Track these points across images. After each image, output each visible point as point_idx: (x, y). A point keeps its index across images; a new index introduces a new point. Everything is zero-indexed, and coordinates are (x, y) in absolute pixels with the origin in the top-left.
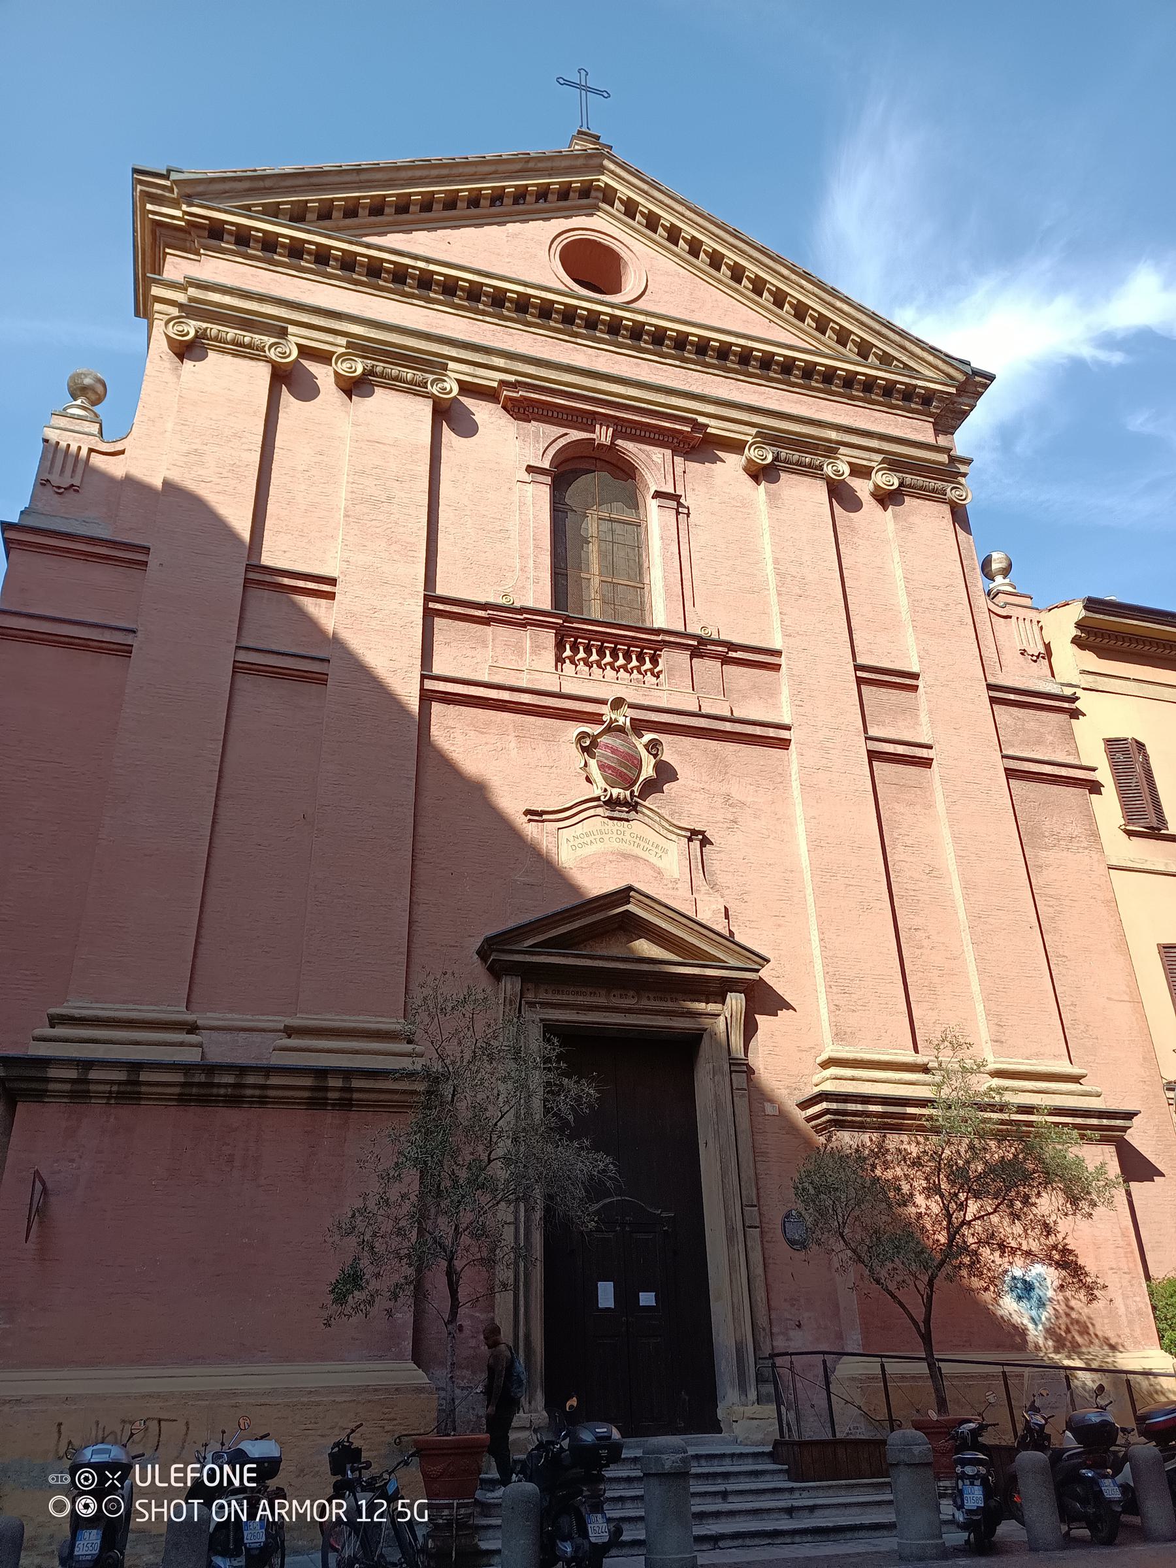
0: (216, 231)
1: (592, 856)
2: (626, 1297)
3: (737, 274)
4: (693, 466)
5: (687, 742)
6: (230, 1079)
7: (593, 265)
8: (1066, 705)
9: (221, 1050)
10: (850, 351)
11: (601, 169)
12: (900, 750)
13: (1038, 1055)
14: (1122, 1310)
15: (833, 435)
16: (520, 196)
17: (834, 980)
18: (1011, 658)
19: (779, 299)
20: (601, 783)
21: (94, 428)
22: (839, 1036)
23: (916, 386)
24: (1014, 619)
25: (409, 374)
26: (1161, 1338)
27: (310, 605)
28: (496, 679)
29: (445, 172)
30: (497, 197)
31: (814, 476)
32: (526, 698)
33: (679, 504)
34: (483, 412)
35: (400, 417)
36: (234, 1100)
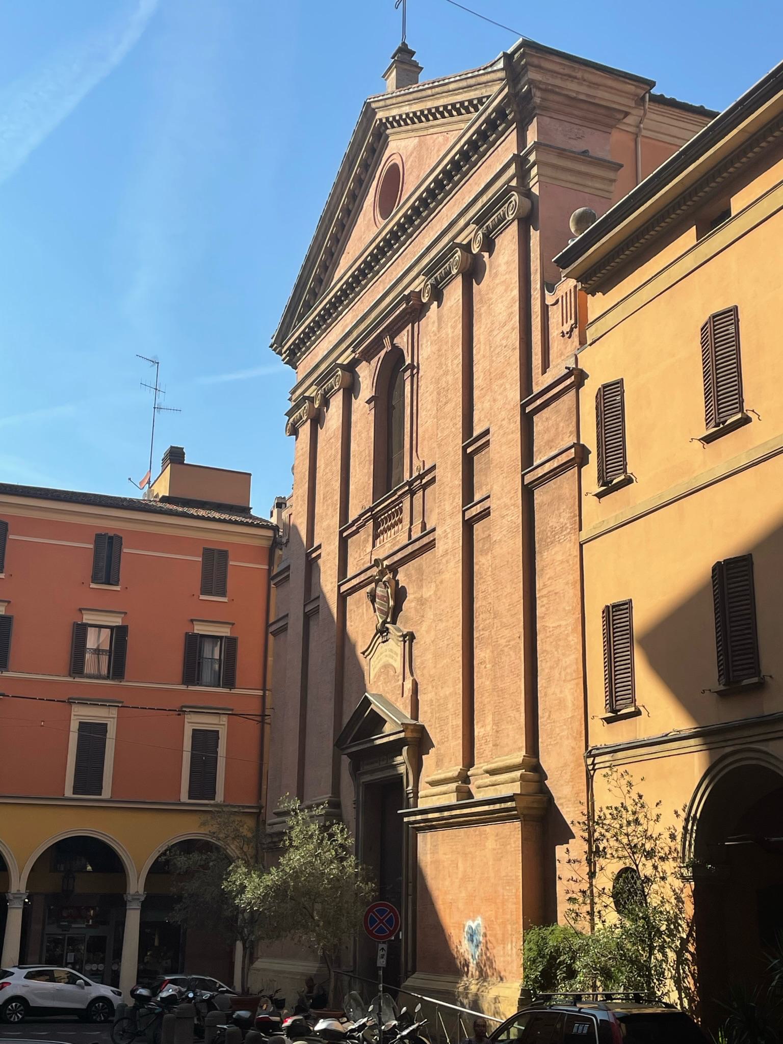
8: (568, 382)
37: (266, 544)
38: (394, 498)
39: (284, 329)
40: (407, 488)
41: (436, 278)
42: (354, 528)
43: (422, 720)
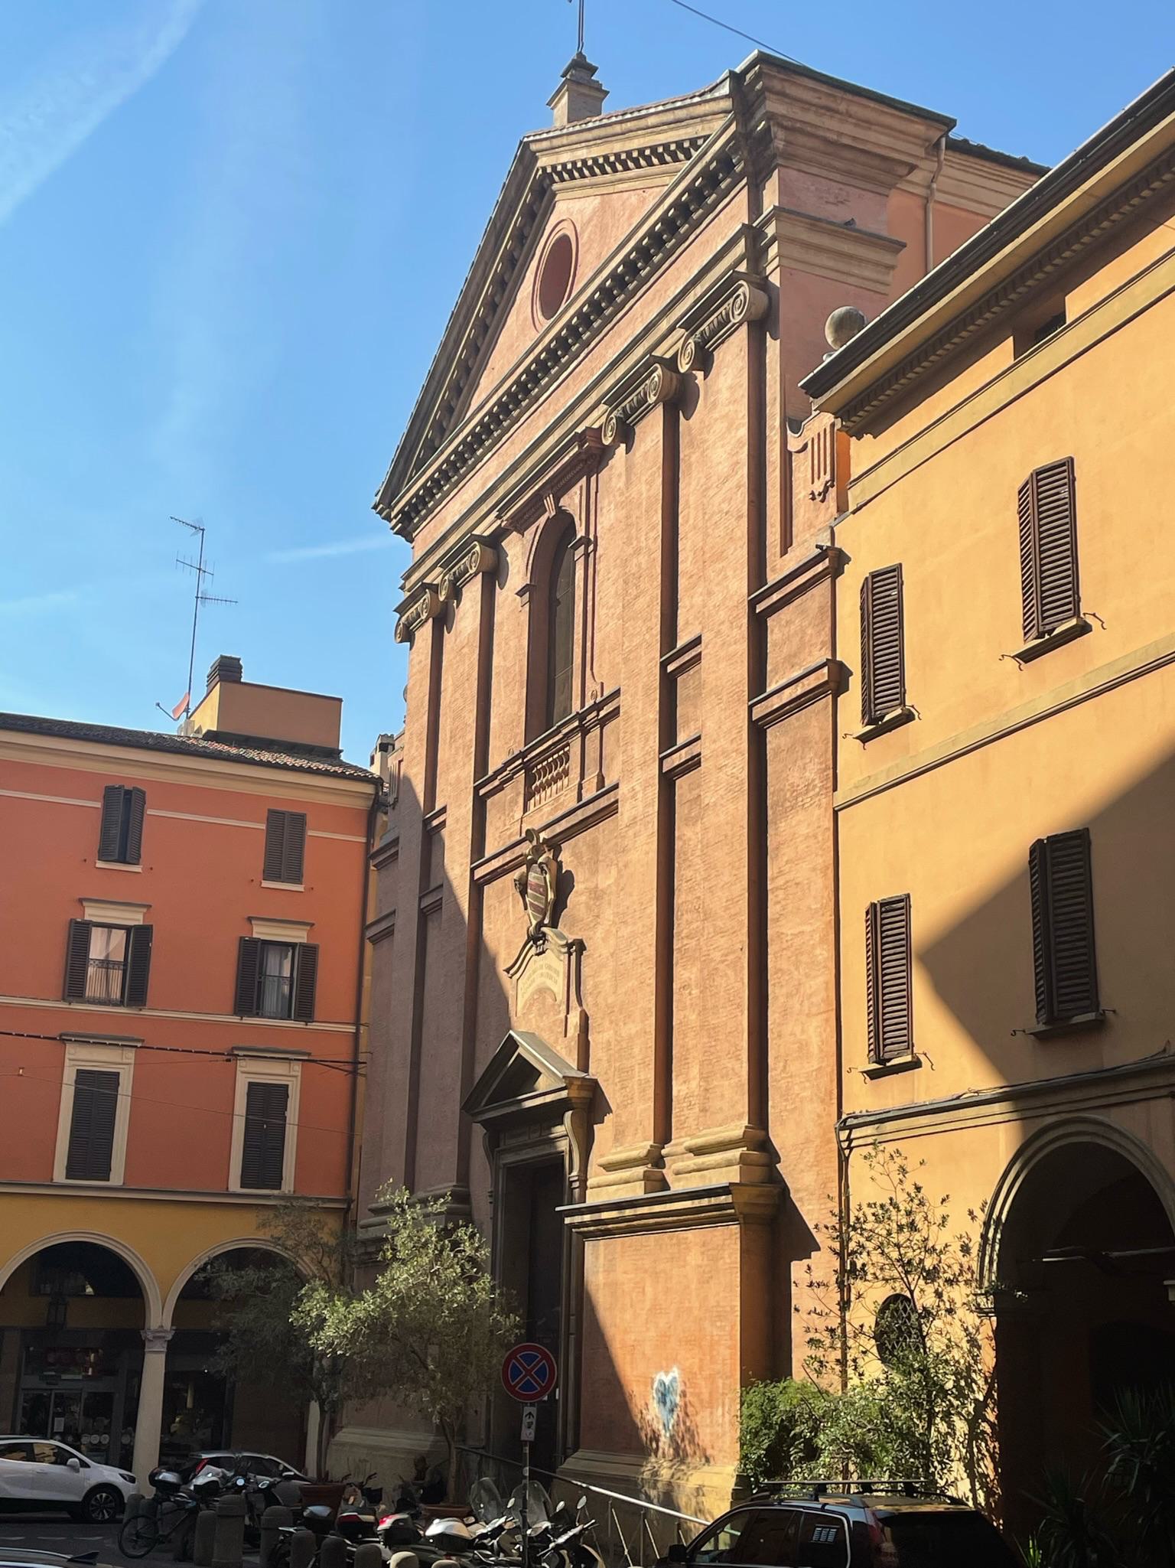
8: (820, 568)
11: (534, 158)
29: (463, 312)
37: (363, 805)
38: (557, 738)
40: (576, 724)
41: (624, 408)
42: (496, 783)
43: (594, 1072)
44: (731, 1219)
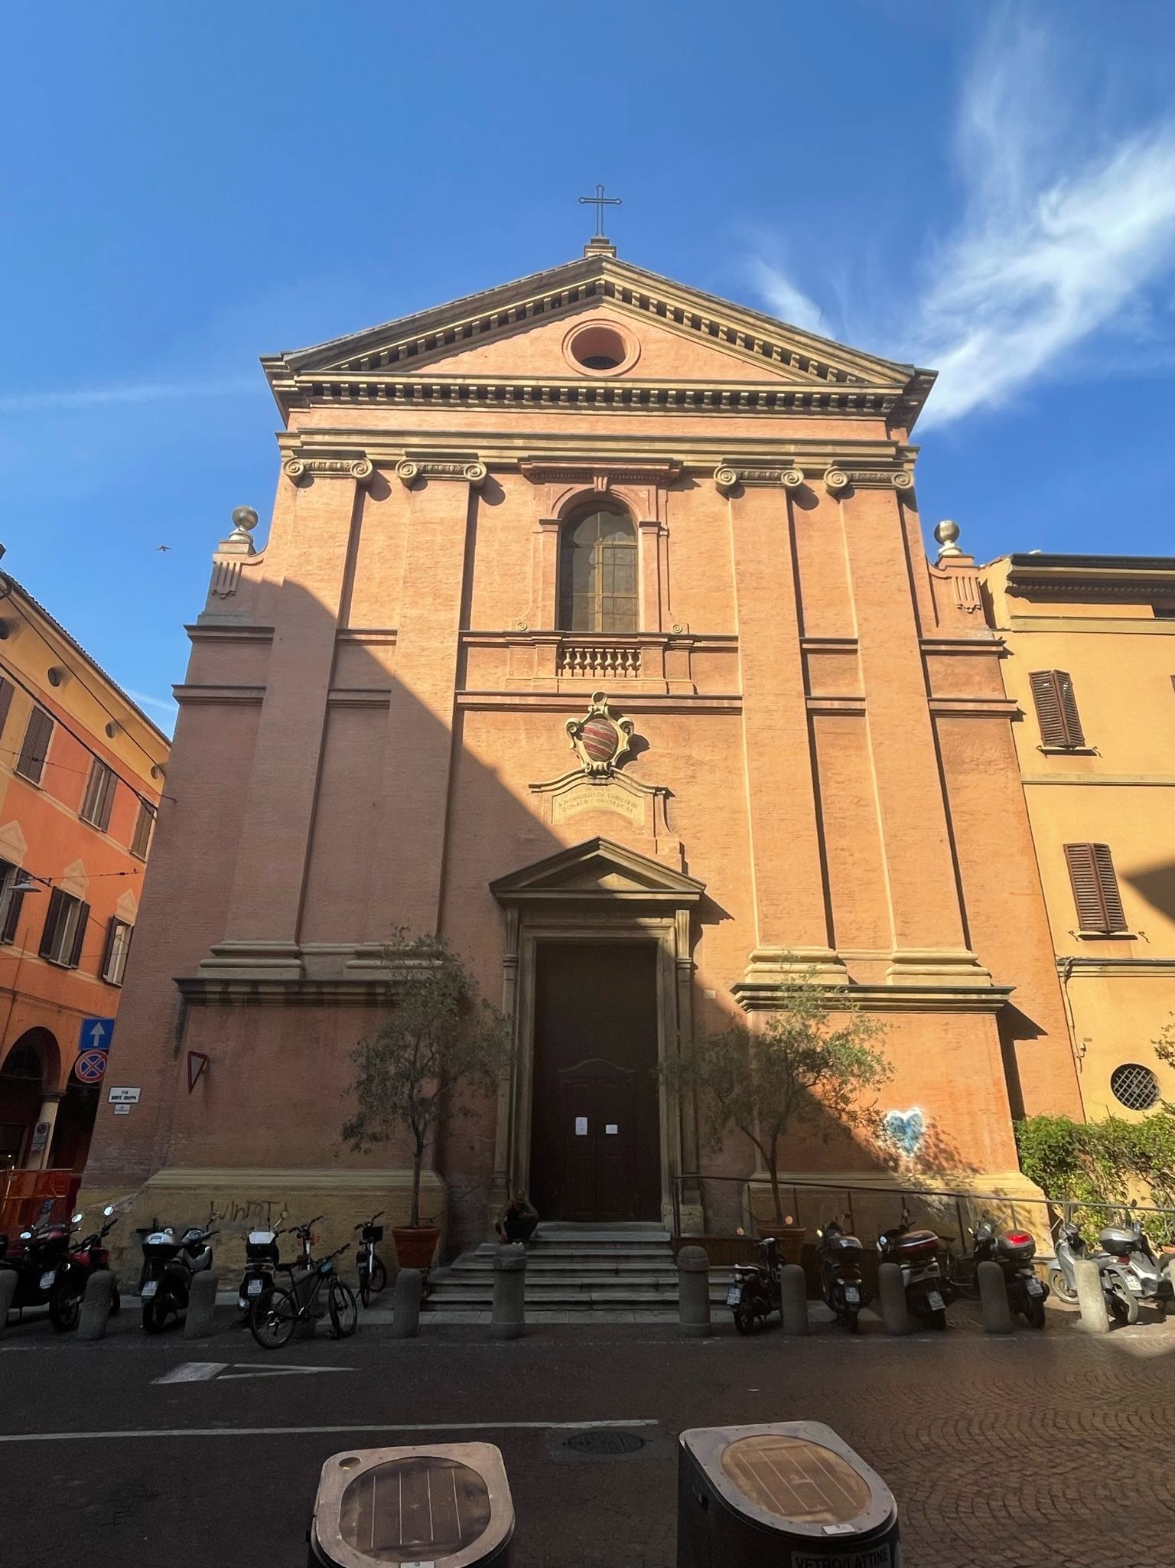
0: (317, 390)
1: (572, 815)
2: (596, 1127)
3: (714, 330)
4: (675, 495)
5: (658, 718)
6: (314, 990)
7: (599, 350)
8: (994, 649)
9: (318, 970)
10: (812, 375)
11: (601, 271)
12: (836, 705)
13: (937, 944)
14: (987, 1142)
15: (792, 448)
16: (539, 307)
17: (766, 894)
18: (947, 613)
19: (749, 343)
20: (587, 758)
21: (245, 548)
22: (766, 938)
23: (865, 395)
24: (953, 580)
25: (451, 466)
26: (1021, 1164)
27: (379, 652)
28: (511, 689)
29: (476, 305)
30: (521, 313)
31: (774, 486)
32: (531, 700)
33: (661, 529)
34: (508, 483)
35: (446, 500)
36: (319, 1003)
39: (317, 358)
44: (990, 1010)
